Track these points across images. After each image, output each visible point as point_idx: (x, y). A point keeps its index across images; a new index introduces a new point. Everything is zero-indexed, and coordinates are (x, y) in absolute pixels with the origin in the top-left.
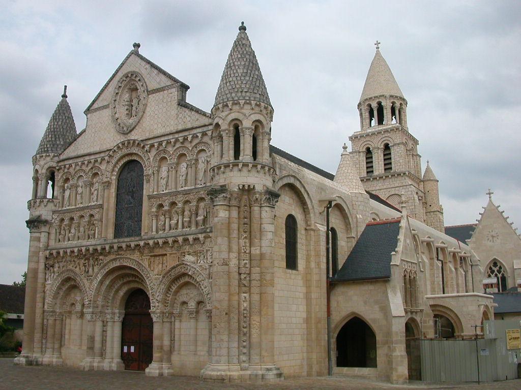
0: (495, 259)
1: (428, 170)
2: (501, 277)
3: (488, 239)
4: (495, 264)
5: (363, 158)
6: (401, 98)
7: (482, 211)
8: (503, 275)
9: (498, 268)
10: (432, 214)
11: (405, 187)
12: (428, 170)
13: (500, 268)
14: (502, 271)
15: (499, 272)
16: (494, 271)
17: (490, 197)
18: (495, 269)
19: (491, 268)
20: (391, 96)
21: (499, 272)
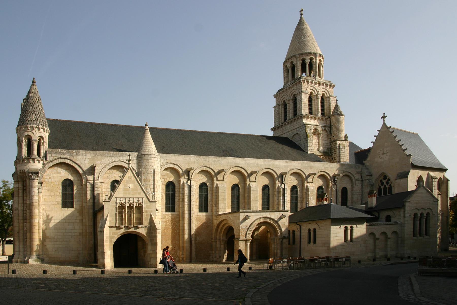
0: (383, 173)
1: (337, 107)
2: (384, 188)
3: (379, 157)
4: (385, 177)
5: (282, 108)
6: (310, 54)
7: (377, 134)
8: (390, 185)
9: (386, 180)
10: (334, 143)
11: (302, 127)
12: (337, 107)
13: (389, 180)
14: (390, 183)
15: (387, 183)
16: (384, 183)
17: (384, 120)
18: (384, 181)
19: (381, 181)
20: (301, 54)
21: (387, 183)
